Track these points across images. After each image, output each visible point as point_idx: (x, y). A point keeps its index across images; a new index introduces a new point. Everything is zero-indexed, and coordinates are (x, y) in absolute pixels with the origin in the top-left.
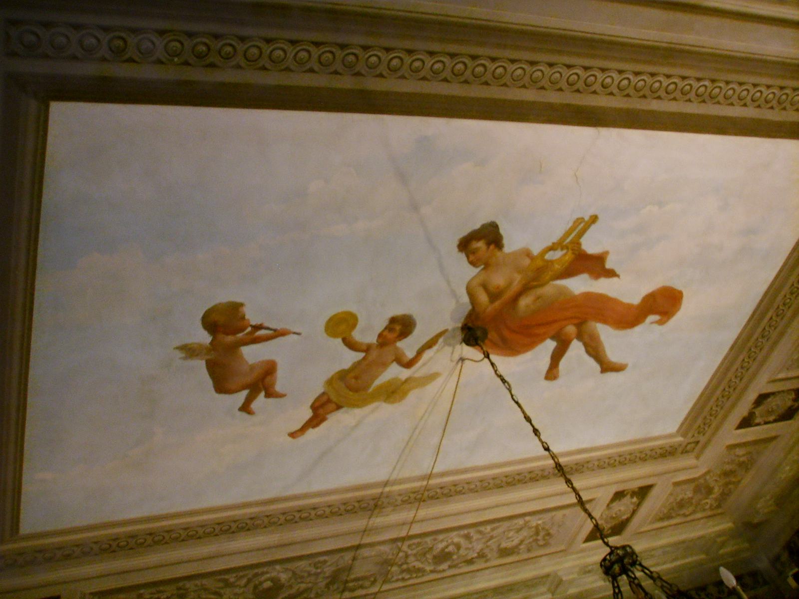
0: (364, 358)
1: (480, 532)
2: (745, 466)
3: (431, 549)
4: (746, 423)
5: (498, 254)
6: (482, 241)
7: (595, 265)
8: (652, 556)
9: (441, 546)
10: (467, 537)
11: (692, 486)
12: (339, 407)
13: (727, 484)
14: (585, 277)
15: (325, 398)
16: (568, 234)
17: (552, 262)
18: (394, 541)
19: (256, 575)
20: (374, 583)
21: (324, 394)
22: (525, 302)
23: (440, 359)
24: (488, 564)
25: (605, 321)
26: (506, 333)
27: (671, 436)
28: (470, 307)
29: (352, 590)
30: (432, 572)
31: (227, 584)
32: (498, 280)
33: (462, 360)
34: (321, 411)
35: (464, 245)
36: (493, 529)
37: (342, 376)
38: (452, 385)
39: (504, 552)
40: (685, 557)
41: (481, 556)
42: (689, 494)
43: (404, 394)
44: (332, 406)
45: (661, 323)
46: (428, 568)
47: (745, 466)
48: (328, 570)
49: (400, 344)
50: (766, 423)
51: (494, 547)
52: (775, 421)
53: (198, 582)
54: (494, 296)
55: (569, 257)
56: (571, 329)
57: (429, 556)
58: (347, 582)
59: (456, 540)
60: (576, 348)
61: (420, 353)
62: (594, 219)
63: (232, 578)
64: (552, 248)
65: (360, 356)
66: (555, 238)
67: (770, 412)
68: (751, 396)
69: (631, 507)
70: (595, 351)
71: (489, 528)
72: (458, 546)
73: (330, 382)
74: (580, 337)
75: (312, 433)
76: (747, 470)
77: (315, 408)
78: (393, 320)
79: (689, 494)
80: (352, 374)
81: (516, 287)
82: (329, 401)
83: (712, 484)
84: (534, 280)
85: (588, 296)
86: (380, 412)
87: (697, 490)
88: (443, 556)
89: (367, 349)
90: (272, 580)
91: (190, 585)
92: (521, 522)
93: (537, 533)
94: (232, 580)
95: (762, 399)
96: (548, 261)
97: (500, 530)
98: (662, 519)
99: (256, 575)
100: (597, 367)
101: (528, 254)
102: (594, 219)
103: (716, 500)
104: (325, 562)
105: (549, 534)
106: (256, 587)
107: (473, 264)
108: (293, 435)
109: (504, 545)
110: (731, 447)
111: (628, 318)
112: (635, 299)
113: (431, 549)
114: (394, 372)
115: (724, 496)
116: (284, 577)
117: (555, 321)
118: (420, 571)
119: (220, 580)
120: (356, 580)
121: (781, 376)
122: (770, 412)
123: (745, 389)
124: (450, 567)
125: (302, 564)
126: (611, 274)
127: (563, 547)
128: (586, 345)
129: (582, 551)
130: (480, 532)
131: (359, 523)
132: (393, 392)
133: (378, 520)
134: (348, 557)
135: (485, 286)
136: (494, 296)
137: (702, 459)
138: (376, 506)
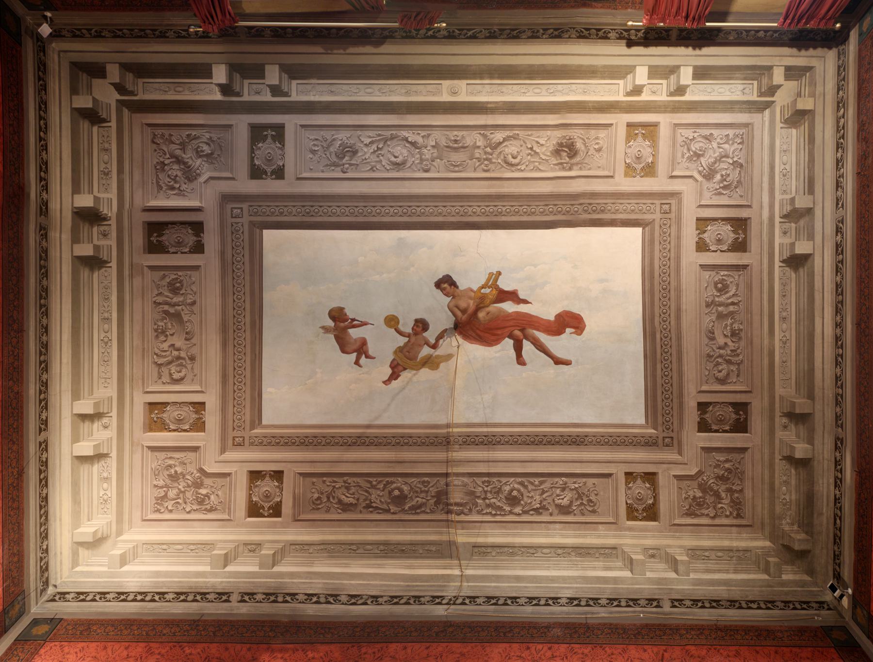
0: (409, 341)
6: (446, 284)
16: (488, 280)
22: (481, 315)
26: (478, 331)
32: (463, 304)
35: (438, 285)
37: (400, 350)
49: (425, 334)
55: (495, 292)
64: (483, 287)
65: (407, 339)
66: (483, 281)
73: (395, 352)
85: (518, 313)
89: (409, 336)
101: (472, 290)
135: (457, 307)
136: (464, 311)
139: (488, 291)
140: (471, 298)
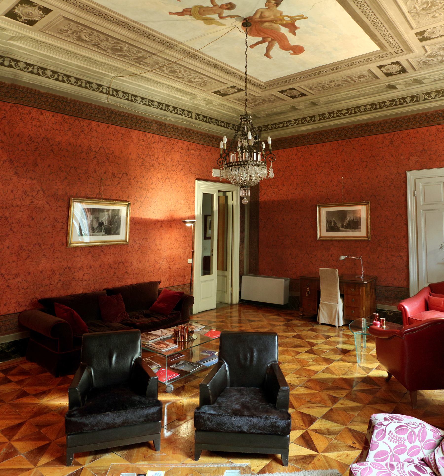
0: (212, 7)
1: (190, 72)
2: (270, 101)
3: (173, 68)
4: (282, 92)
5: (275, 8)
7: (292, 28)
8: (224, 107)
9: (176, 68)
10: (185, 71)
11: (253, 97)
12: (191, 15)
13: (261, 103)
14: (288, 29)
15: (189, 10)
17: (284, 20)
18: (166, 59)
19: (118, 43)
20: (148, 66)
21: (191, 8)
22: (267, 24)
23: (229, 22)
24: (183, 82)
25: (279, 44)
27: (262, 82)
28: (252, 15)
29: (140, 64)
30: (166, 74)
31: (107, 40)
32: (267, 14)
33: (236, 27)
34: (185, 12)
36: (194, 74)
37: (201, 7)
38: (226, 31)
39: (190, 81)
40: (231, 113)
41: (183, 78)
42: (250, 99)
43: (212, 24)
44: (189, 13)
45: (291, 54)
46: (166, 72)
47: (270, 101)
48: (139, 55)
49: (225, 11)
50: (287, 95)
51: (189, 78)
52: (289, 96)
53: (99, 34)
54: (261, 17)
56: (269, 39)
57: (170, 69)
58: (141, 61)
59: (181, 70)
60: (266, 45)
61: (227, 17)
62: (306, 18)
63: (110, 39)
64: (288, 17)
65: (212, 6)
67: (290, 93)
68: (291, 87)
69: (233, 92)
70: (268, 49)
71: (193, 72)
72: (180, 72)
73: (196, 7)
74: (269, 43)
75: (176, 16)
76: (270, 103)
77: (184, 10)
78: (230, 4)
79: (250, 99)
80: (204, 9)
81: (269, 19)
82: (190, 11)
83: (258, 100)
84: (275, 21)
86: (200, 23)
87: (252, 99)
88: (174, 72)
89: (215, 6)
90: (121, 47)
91: (96, 33)
92: (203, 76)
93: (203, 82)
94: (110, 40)
95: (293, 89)
96: (283, 19)
97: (196, 75)
98: (236, 100)
99: (118, 43)
100: (265, 53)
102: (306, 18)
103: (254, 104)
104: (141, 52)
105: (206, 84)
106: (114, 46)
107: (266, 5)
108: (170, 13)
109: (192, 79)
110: (272, 95)
111: (285, 46)
112: (292, 44)
113: (173, 68)
114: (216, 16)
115: (258, 105)
116: (125, 48)
117: (268, 34)
118: (163, 71)
119: (106, 38)
120: (144, 62)
121: (302, 87)
122: (290, 93)
123: (291, 84)
124: (172, 76)
125: (134, 48)
126: (294, 34)
127: (205, 90)
128: (268, 46)
129: (209, 94)
130: (190, 72)
131: (161, 48)
132: (209, 21)
133: (167, 51)
134: (149, 55)
135: (262, 13)
137: (262, 93)
138: (171, 47)
139: (288, 19)
140: (274, 15)
